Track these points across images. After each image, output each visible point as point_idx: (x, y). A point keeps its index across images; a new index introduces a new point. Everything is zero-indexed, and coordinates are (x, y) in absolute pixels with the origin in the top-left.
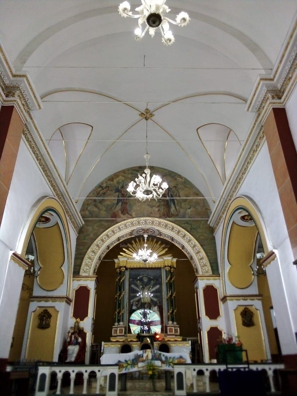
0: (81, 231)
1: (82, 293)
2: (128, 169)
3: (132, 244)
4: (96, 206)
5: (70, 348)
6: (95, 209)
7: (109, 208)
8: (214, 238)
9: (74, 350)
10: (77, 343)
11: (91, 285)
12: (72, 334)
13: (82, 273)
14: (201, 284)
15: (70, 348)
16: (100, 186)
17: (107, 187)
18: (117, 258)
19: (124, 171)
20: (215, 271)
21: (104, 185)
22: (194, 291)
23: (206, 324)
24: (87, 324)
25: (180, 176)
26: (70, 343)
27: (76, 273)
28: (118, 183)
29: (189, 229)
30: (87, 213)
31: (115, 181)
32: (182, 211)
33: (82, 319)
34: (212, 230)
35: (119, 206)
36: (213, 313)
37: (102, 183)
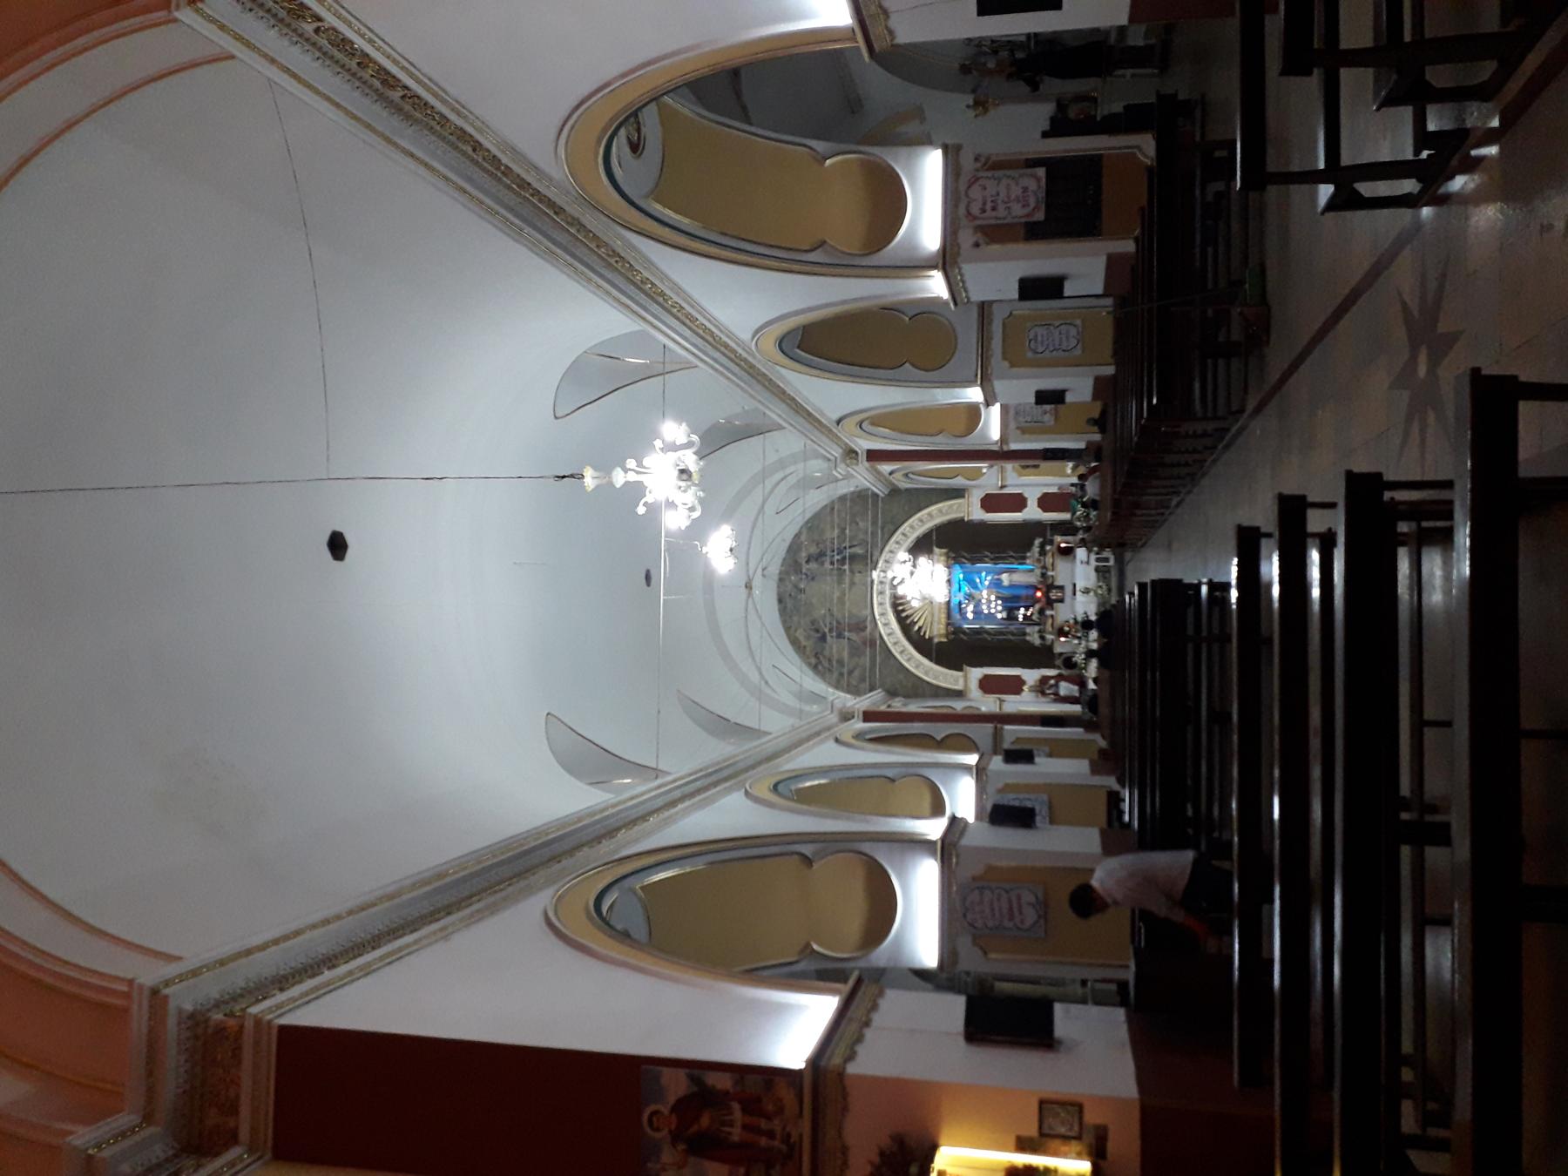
0: (892, 693)
1: (987, 685)
2: (784, 622)
3: (908, 617)
4: (850, 672)
5: (1062, 692)
6: (856, 673)
7: (855, 651)
8: (907, 490)
9: (1065, 688)
10: (1056, 685)
11: (976, 673)
12: (1043, 693)
13: (959, 687)
14: (978, 514)
15: (1062, 692)
16: (815, 668)
17: (816, 655)
18: (931, 639)
19: (787, 629)
20: (958, 493)
21: (813, 661)
22: (982, 525)
23: (1032, 512)
24: (1031, 676)
25: (797, 536)
26: (1056, 694)
27: (959, 694)
28: (808, 638)
29: (892, 528)
30: (862, 686)
31: (804, 643)
32: (861, 536)
33: (1023, 683)
34: (895, 492)
35: (854, 636)
36: (1018, 502)
37: (809, 664)
